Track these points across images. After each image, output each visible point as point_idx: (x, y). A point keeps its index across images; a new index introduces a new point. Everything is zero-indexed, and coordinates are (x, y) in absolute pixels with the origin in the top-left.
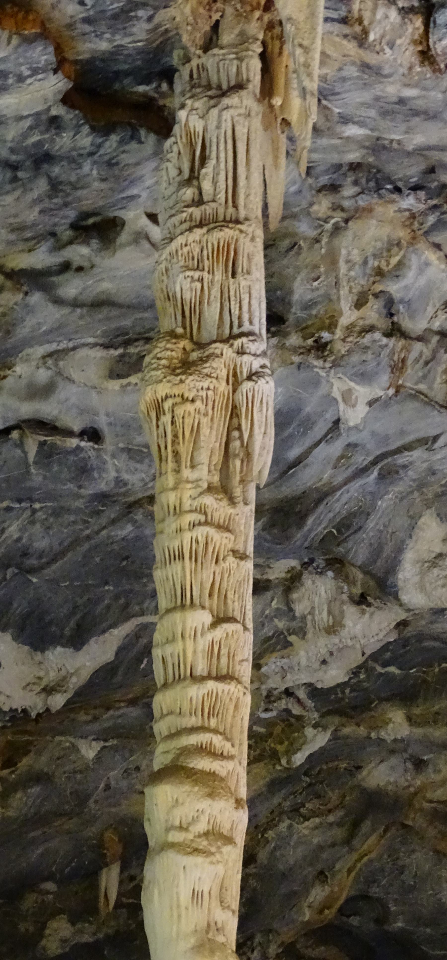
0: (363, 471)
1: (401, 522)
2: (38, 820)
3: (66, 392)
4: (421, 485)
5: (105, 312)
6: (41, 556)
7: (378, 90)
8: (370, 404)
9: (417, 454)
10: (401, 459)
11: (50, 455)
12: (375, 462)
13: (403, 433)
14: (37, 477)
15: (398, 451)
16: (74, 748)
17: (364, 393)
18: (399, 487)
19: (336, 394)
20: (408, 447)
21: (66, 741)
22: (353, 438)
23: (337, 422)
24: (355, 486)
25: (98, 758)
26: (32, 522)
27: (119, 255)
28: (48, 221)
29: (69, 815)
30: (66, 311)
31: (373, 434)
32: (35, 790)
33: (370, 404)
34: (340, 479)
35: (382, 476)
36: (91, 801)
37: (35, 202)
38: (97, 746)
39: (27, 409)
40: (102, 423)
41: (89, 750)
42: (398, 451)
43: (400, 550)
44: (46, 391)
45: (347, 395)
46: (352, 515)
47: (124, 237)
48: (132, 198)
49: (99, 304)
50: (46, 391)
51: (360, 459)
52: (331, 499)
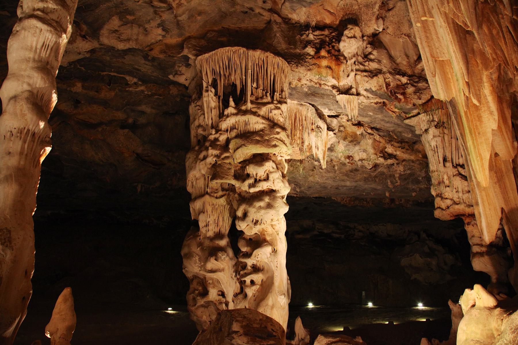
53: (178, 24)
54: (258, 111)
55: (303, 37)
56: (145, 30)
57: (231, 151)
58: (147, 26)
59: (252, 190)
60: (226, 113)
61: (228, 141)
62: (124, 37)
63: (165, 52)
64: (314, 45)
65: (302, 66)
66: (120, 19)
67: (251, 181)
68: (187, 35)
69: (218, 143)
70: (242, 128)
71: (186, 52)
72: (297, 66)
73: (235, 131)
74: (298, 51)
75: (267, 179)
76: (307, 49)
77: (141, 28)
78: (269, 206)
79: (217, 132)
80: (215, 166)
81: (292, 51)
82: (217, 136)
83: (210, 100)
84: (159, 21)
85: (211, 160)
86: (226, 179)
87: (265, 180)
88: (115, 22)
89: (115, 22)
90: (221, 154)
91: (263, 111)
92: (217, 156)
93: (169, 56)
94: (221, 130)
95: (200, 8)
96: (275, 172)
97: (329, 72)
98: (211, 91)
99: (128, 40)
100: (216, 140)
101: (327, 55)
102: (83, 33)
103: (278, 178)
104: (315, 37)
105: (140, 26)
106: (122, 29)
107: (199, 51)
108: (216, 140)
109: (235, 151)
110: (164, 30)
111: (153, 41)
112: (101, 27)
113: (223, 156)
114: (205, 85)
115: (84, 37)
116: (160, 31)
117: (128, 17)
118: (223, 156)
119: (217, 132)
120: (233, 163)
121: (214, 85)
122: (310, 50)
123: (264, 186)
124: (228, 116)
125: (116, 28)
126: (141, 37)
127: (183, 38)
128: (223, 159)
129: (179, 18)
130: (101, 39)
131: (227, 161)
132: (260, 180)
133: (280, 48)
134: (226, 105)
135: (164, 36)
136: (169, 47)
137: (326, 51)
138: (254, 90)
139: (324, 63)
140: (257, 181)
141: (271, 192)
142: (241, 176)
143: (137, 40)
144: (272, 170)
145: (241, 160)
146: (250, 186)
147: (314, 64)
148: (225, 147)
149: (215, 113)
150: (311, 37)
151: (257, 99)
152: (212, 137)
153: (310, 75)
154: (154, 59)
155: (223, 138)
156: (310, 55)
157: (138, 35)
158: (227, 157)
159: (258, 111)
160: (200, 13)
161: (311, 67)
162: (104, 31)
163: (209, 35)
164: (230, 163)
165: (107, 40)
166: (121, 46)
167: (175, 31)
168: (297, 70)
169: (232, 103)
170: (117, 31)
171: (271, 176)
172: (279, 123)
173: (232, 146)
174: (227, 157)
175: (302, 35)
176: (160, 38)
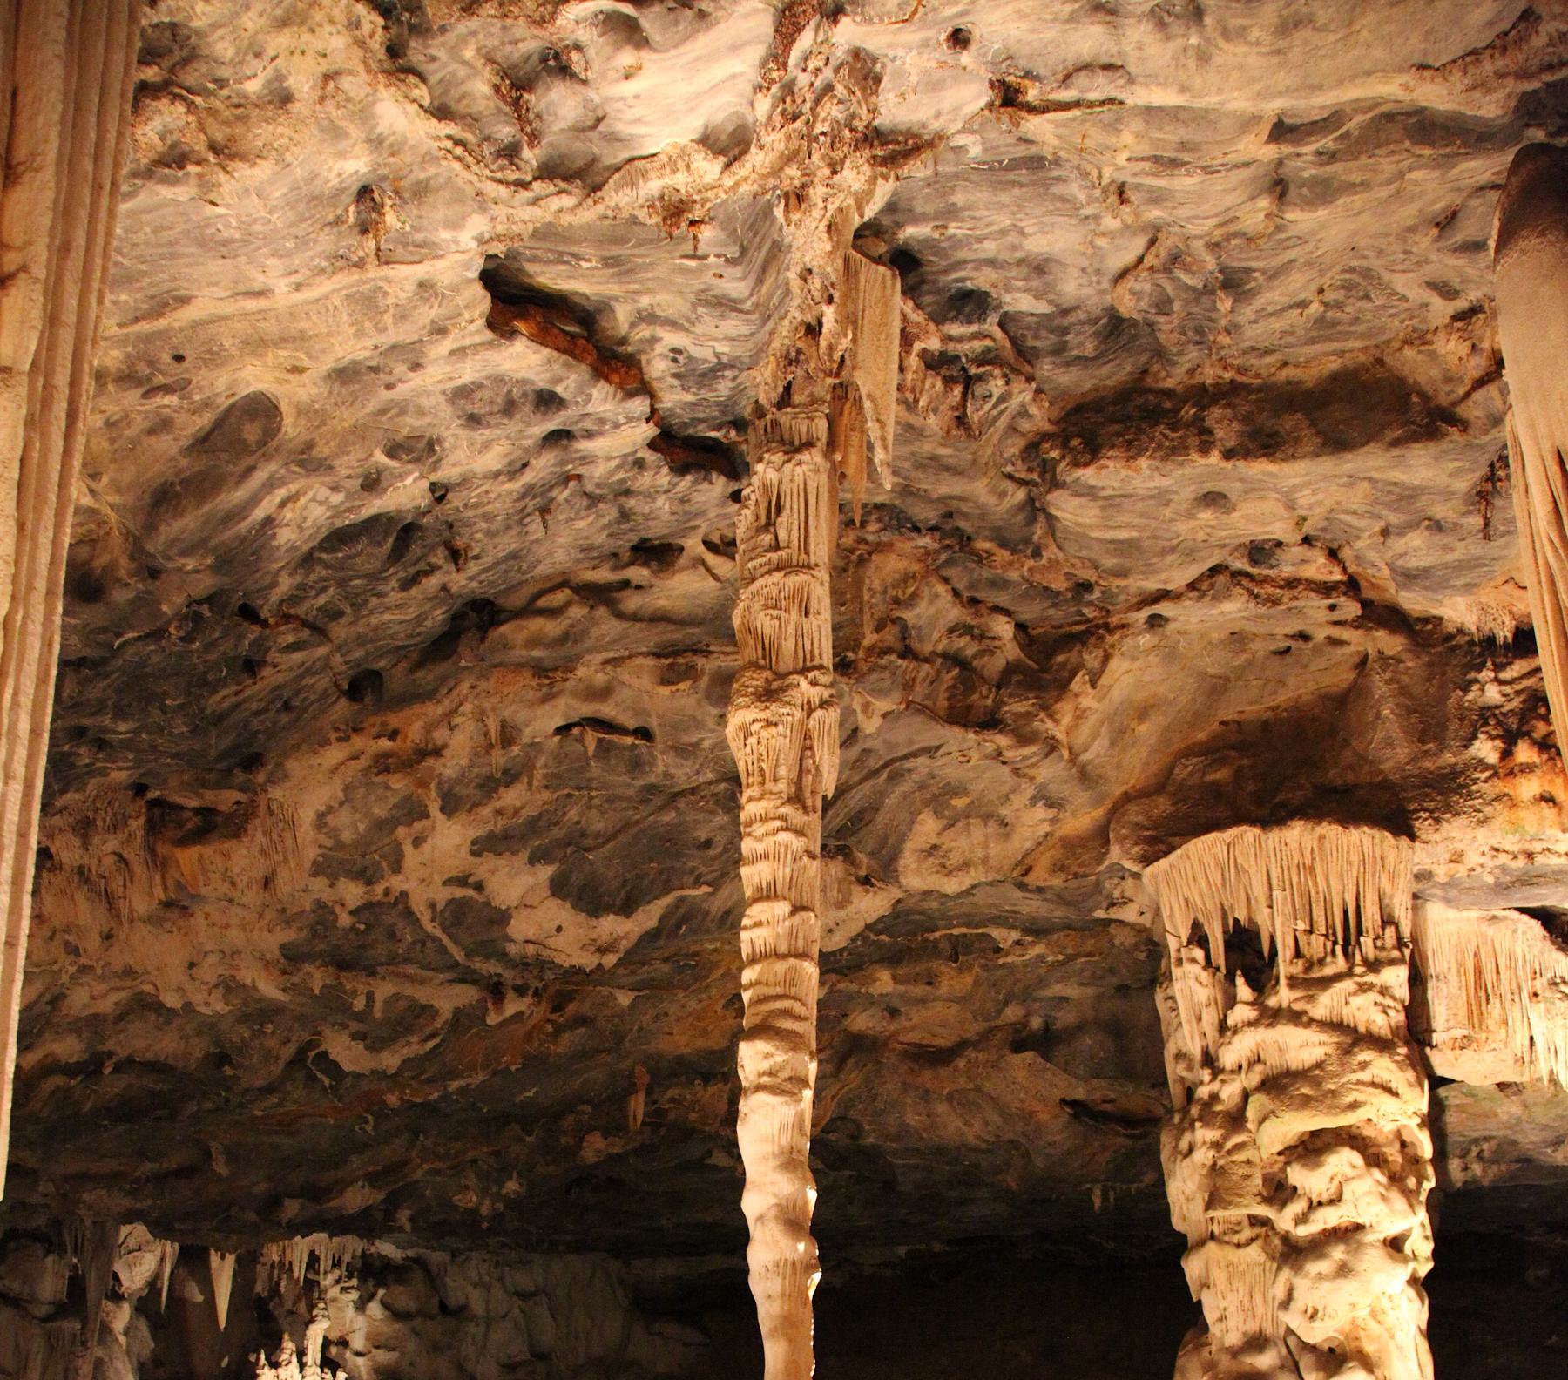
0: (875, 773)
1: (904, 816)
2: (582, 1055)
3: (623, 695)
4: (922, 787)
5: (662, 627)
6: (598, 835)
7: (916, 447)
8: (884, 716)
9: (921, 760)
10: (908, 764)
11: (607, 750)
12: (884, 767)
13: (911, 742)
14: (595, 770)
15: (906, 757)
16: (612, 997)
17: (882, 705)
18: (905, 787)
19: (856, 706)
20: (915, 755)
21: (605, 990)
22: (869, 744)
23: (855, 730)
24: (867, 786)
25: (633, 1006)
26: (590, 808)
27: (678, 577)
28: (612, 545)
29: (608, 1051)
30: (626, 625)
31: (885, 742)
32: (581, 1031)
33: (884, 716)
34: (856, 778)
35: (890, 778)
36: (627, 1044)
37: (605, 527)
38: (633, 995)
39: (588, 709)
40: (653, 724)
41: (624, 999)
42: (906, 757)
43: (902, 840)
44: (604, 693)
45: (866, 707)
46: (862, 811)
47: (683, 561)
48: (694, 528)
49: (659, 618)
50: (604, 693)
51: (873, 763)
52: (848, 796)
53: (1085, 776)
54: (1308, 1007)
55: (1470, 696)
56: (1003, 823)
57: (1250, 1125)
58: (1003, 811)
59: (1302, 1231)
60: (1230, 1022)
61: (1246, 1095)
62: (954, 859)
63: (1063, 868)
64: (1499, 723)
65: (1457, 814)
66: (938, 814)
67: (1297, 1207)
68: (1117, 791)
69: (1219, 1108)
70: (1274, 1061)
71: (1115, 854)
72: (1438, 821)
73: (1258, 1068)
74: (1448, 758)
75: (1335, 1201)
76: (1477, 743)
77: (991, 822)
78: (1343, 1270)
79: (1214, 1076)
80: (1215, 1170)
81: (1427, 764)
82: (1215, 1086)
83: (1191, 987)
84: (1030, 791)
85: (1203, 1156)
86: (1237, 1205)
87: (1332, 1202)
88: (927, 827)
89: (927, 827)
90: (1225, 1138)
91: (1325, 1004)
92: (1217, 1146)
93: (1076, 876)
94: (1222, 1071)
95: (1140, 696)
96: (1359, 1177)
97: (1547, 811)
98: (1193, 961)
99: (966, 865)
100: (1215, 1097)
101: (1537, 760)
102: (863, 873)
103: (1369, 1193)
104: (1507, 689)
105: (986, 818)
106: (947, 841)
107: (1149, 841)
108: (1215, 1097)
109: (1260, 1123)
110: (1050, 805)
111: (1028, 845)
112: (894, 857)
113: (1228, 1145)
114: (1172, 944)
115: (866, 881)
116: (1040, 812)
117: (954, 802)
118: (1228, 1145)
119: (1214, 1076)
120: (1256, 1160)
121: (1198, 937)
122: (1486, 749)
123: (1329, 1218)
124: (1236, 1031)
125: (934, 841)
126: (995, 850)
127: (1108, 804)
128: (1229, 1152)
129: (1085, 757)
130: (904, 881)
131: (1240, 1157)
132: (1320, 1204)
133: (1390, 764)
134: (1231, 1001)
135: (1054, 821)
136: (1071, 845)
137: (1534, 742)
138: (1302, 939)
139: (1528, 787)
140: (1314, 1206)
141: (1349, 1233)
142: (1279, 1192)
143: (985, 861)
144: (1350, 1172)
145: (1279, 1148)
146: (1302, 1219)
147: (1498, 799)
148: (1236, 1120)
149: (1210, 1018)
150: (1493, 694)
151: (1308, 969)
152: (1203, 1092)
153: (1484, 837)
154: (1040, 890)
155: (1229, 1092)
156: (1487, 767)
157: (986, 845)
158: (1240, 1147)
159: (1308, 1007)
160: (1143, 713)
161: (1488, 810)
162: (908, 860)
163: (1180, 773)
164: (1248, 1162)
165: (916, 877)
166: (952, 886)
167: (1081, 797)
168: (1437, 837)
169: (1244, 991)
170: (935, 847)
171: (1347, 1190)
172: (1375, 1029)
173: (1251, 1113)
174: (1240, 1147)
175: (1466, 690)
176: (1046, 828)
